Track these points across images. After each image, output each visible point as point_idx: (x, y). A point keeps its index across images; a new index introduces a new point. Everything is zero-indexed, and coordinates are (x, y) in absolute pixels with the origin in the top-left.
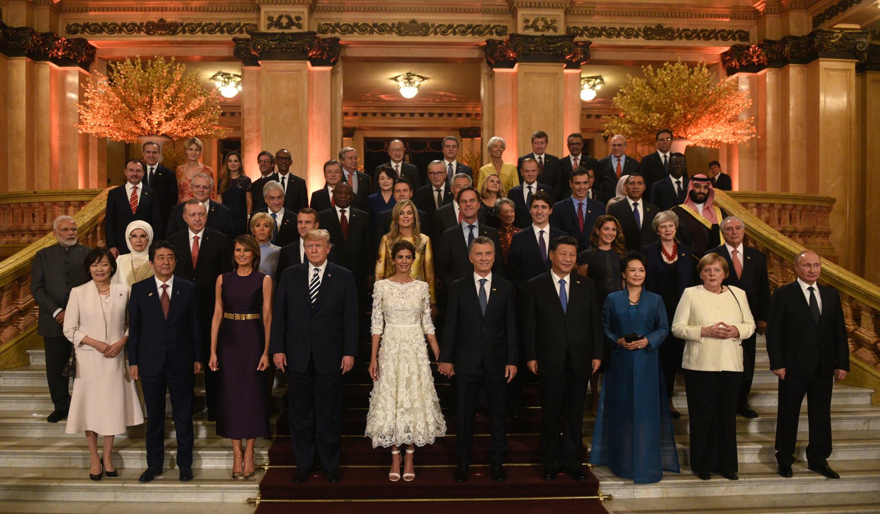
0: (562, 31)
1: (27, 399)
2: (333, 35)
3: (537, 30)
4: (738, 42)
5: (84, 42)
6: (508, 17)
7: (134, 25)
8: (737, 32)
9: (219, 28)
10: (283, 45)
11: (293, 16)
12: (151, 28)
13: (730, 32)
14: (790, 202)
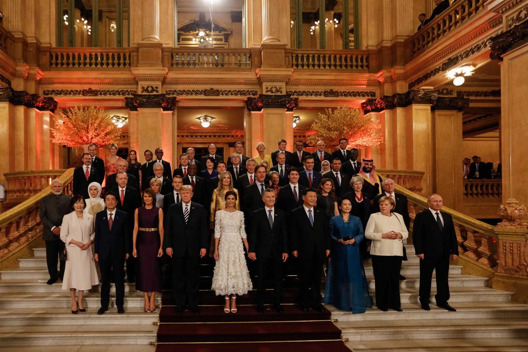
0: (284, 93)
1: (35, 273)
2: (173, 96)
3: (272, 92)
4: (370, 97)
5: (52, 99)
6: (258, 87)
7: (77, 91)
9: (118, 93)
10: (150, 100)
11: (154, 87)
12: (85, 93)
13: (366, 93)
14: (403, 174)
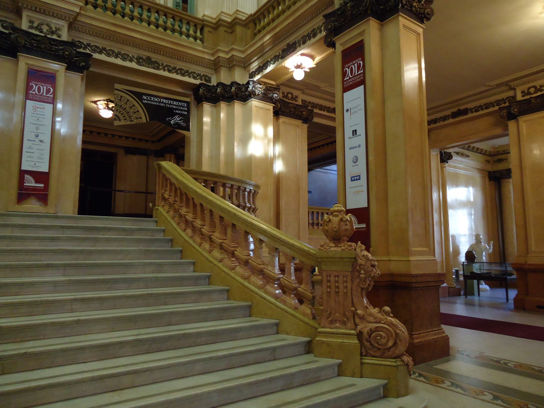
4: (204, 82)
8: (203, 76)
